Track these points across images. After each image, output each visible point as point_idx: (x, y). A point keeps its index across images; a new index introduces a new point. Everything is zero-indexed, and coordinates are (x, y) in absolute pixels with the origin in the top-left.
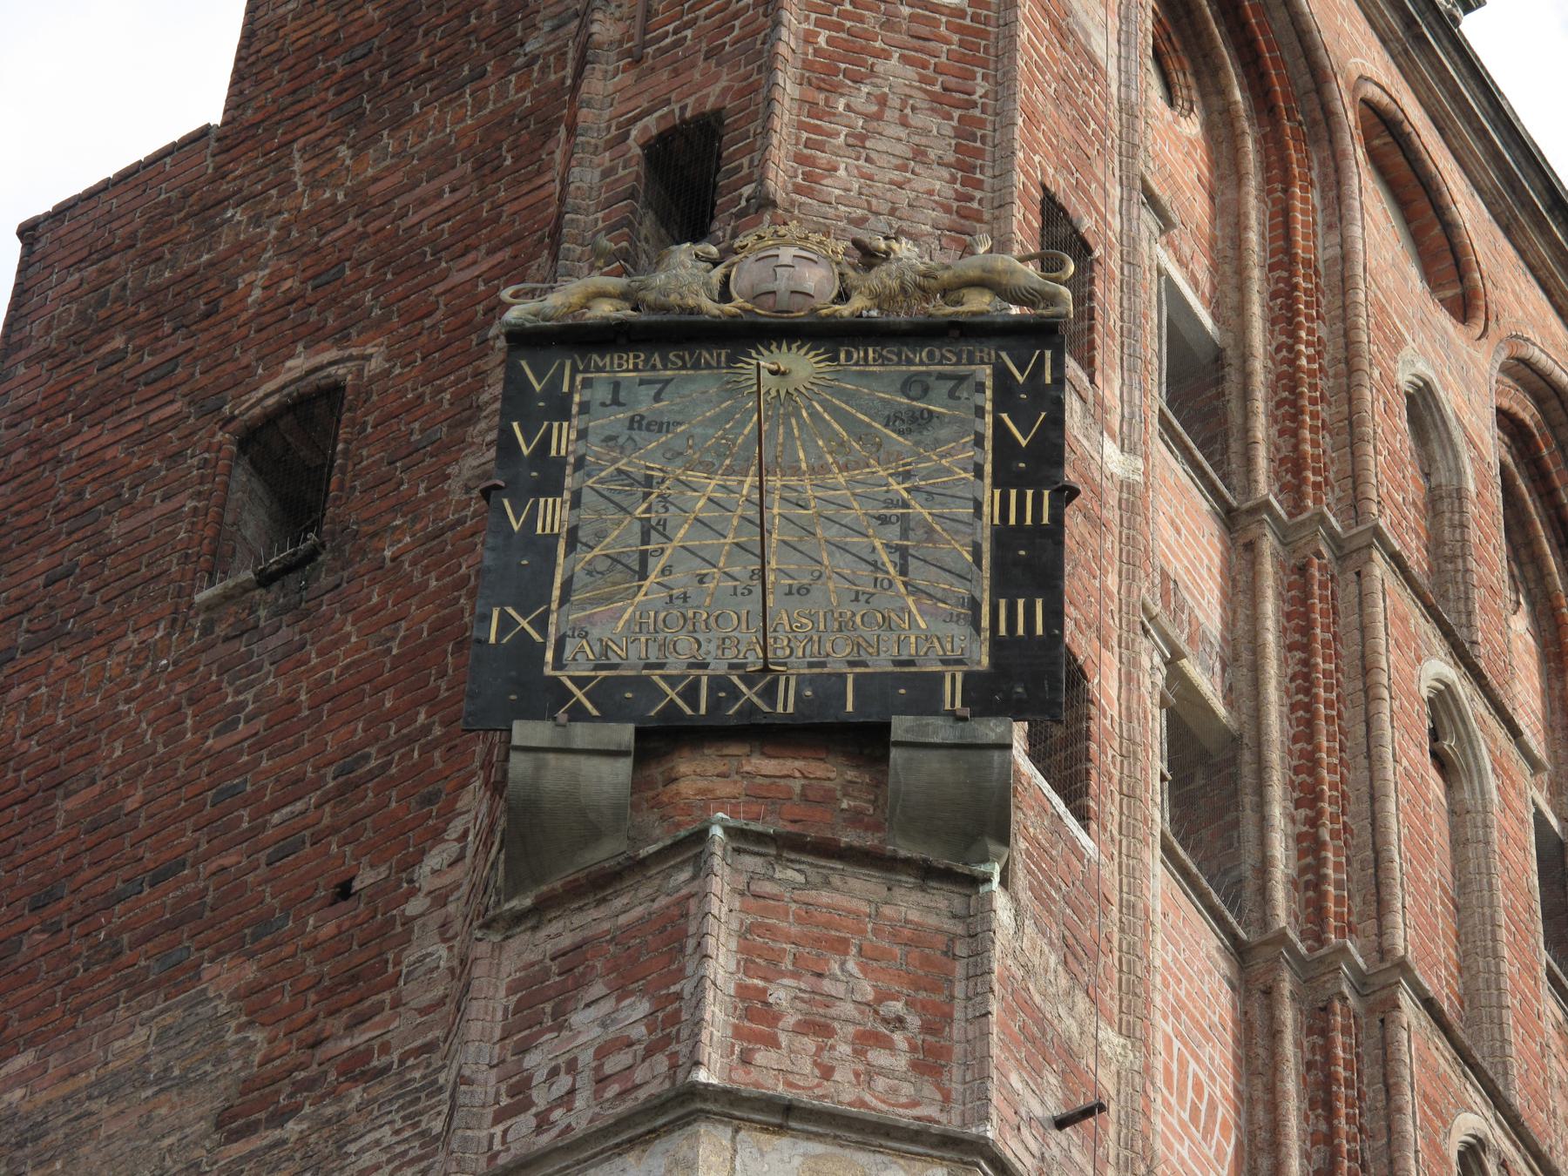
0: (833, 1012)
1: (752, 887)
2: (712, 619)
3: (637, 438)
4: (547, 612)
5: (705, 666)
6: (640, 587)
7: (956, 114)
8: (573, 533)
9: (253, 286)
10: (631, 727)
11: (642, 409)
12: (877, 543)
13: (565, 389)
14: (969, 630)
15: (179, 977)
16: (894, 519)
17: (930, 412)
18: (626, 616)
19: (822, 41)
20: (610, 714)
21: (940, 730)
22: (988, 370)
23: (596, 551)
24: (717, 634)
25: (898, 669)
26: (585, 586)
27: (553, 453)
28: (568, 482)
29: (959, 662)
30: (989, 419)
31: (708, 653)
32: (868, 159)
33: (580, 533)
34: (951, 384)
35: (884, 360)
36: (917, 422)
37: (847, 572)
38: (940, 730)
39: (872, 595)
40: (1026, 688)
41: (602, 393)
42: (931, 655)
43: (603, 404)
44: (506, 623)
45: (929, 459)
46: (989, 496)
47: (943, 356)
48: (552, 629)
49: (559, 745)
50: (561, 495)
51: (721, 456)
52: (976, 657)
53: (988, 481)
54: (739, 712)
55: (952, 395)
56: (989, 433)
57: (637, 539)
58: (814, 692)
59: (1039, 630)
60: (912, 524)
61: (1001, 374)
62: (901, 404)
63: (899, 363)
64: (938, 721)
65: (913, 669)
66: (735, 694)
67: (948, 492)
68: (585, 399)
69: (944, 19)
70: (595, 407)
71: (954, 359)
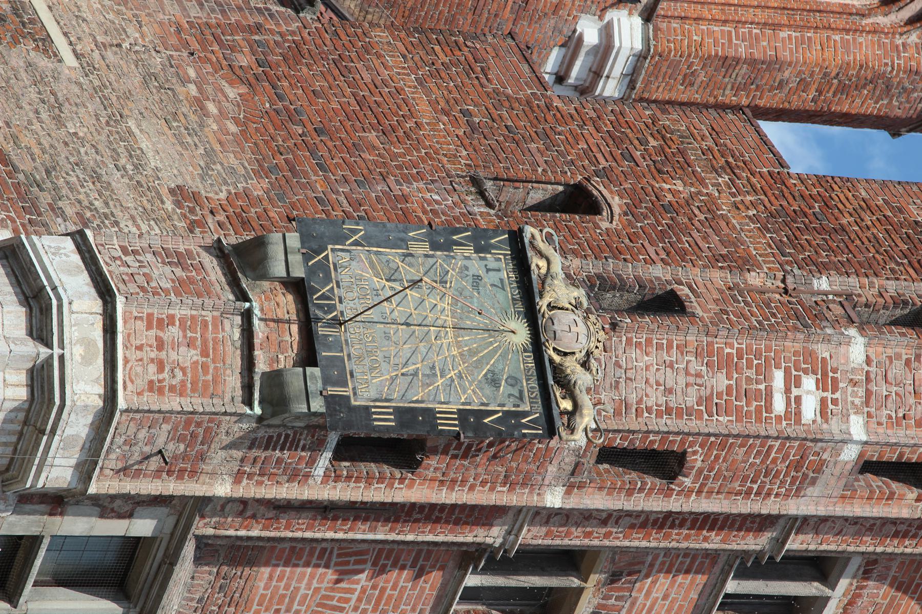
0: (170, 350)
4: (364, 246)
5: (341, 302)
7: (703, 408)
8: (411, 255)
9: (675, 187)
11: (486, 280)
15: (262, 171)
17: (500, 387)
19: (728, 350)
21: (315, 385)
22: (528, 408)
23: (400, 264)
28: (439, 253)
29: (355, 394)
32: (658, 370)
34: (517, 395)
35: (527, 370)
36: (493, 381)
38: (315, 385)
41: (492, 264)
43: (486, 266)
45: (471, 386)
46: (454, 408)
47: (532, 393)
48: (354, 248)
53: (461, 407)
55: (510, 395)
59: (375, 423)
61: (525, 414)
63: (526, 375)
64: (320, 385)
65: (349, 377)
67: (452, 392)
69: (763, 403)
70: (485, 262)
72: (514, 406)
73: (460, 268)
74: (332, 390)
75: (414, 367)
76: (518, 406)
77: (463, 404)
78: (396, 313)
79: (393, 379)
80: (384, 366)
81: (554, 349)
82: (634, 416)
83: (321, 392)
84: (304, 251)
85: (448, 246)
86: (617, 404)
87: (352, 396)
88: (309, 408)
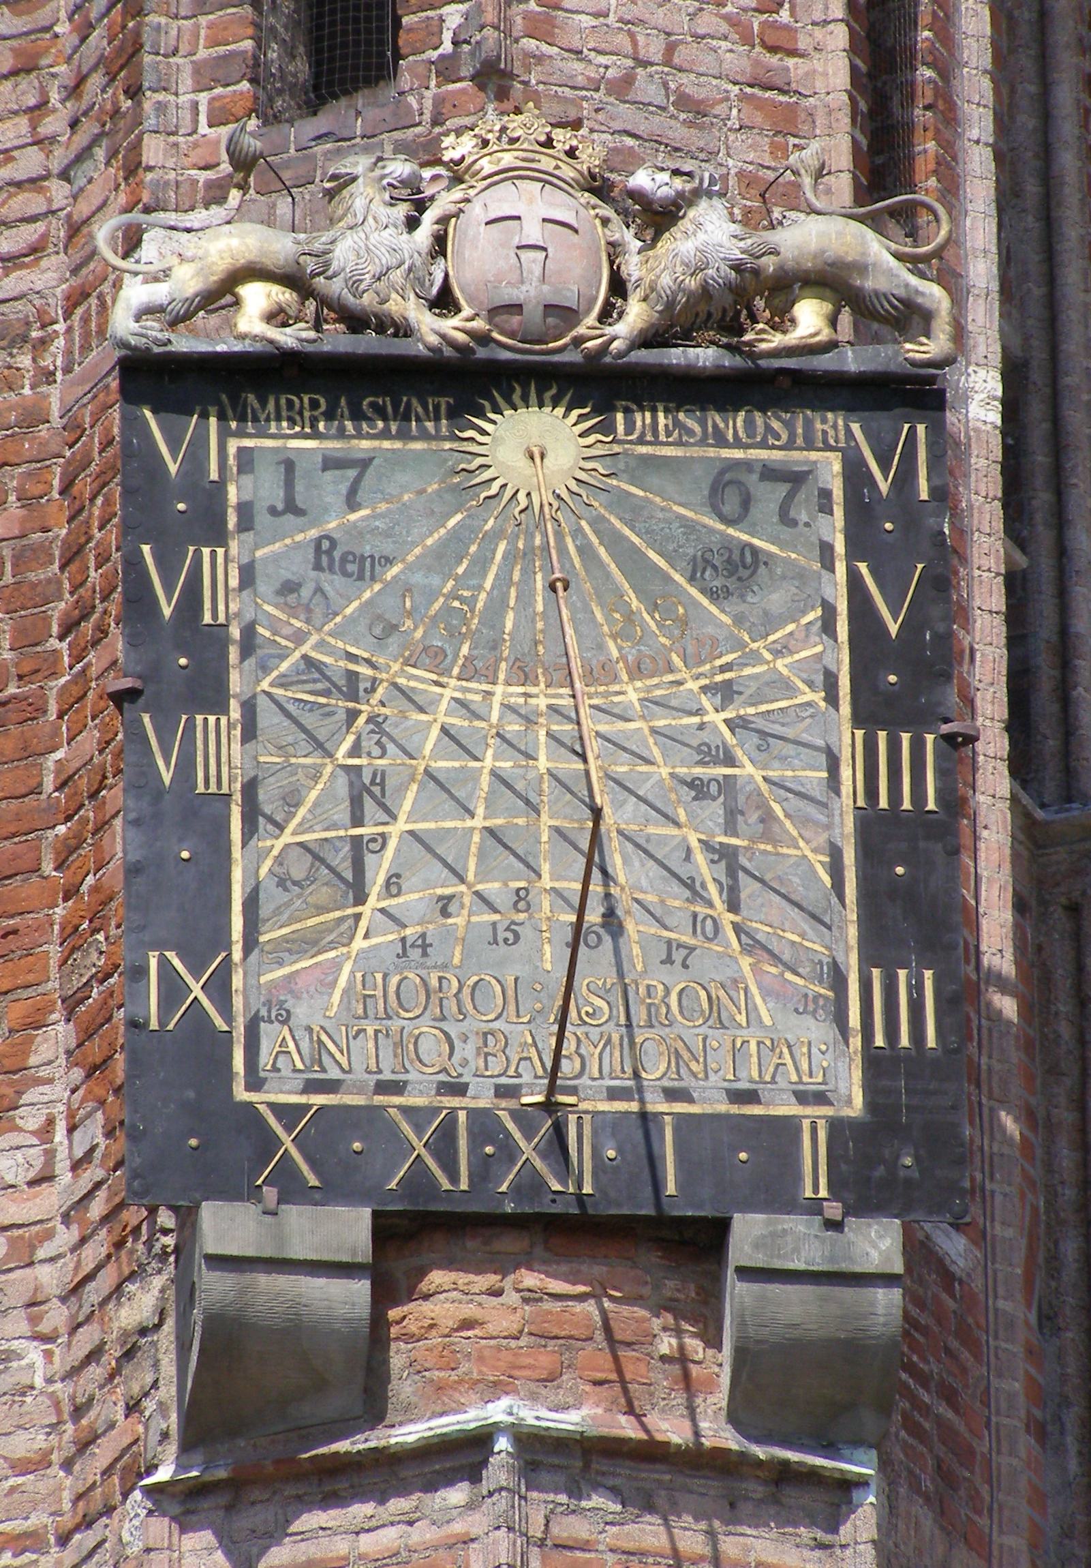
1: (555, 1530)
2: (466, 991)
3: (327, 588)
5: (459, 1089)
6: (358, 917)
8: (250, 789)
10: (367, 1212)
12: (693, 839)
13: (214, 476)
14: (832, 1032)
16: (714, 788)
17: (755, 551)
18: (342, 982)
20: (335, 1189)
21: (801, 1242)
23: (287, 838)
24: (474, 1024)
25: (735, 1109)
26: (277, 911)
27: (207, 618)
28: (235, 681)
30: (841, 568)
31: (465, 1063)
33: (262, 795)
34: (783, 489)
35: (682, 436)
36: (734, 571)
37: (650, 898)
38: (801, 1242)
39: (692, 949)
40: (917, 1159)
42: (782, 1083)
44: (172, 989)
46: (847, 738)
47: (768, 428)
48: (238, 1002)
49: (267, 1253)
50: (226, 711)
51: (455, 636)
52: (843, 1091)
53: (846, 708)
54: (517, 1190)
55: (786, 518)
56: (842, 607)
57: (342, 812)
58: (619, 1150)
59: (931, 1041)
60: (741, 799)
61: (855, 474)
62: (712, 531)
63: (703, 442)
64: (798, 1225)
65: (757, 1110)
66: (509, 1151)
67: (789, 732)
68: (247, 497)
70: (262, 519)
71: (785, 437)
72: (826, 507)
73: (292, 611)
74: (815, 1181)
75: (700, 858)
76: (826, 494)
77: (832, 699)
78: (490, 888)
79: (753, 945)
80: (705, 965)
81: (606, 315)
82: (791, 62)
83: (834, 1225)
84: (270, 1193)
85: (206, 645)
86: (758, 118)
87: (828, 1111)
88: (888, 1280)
